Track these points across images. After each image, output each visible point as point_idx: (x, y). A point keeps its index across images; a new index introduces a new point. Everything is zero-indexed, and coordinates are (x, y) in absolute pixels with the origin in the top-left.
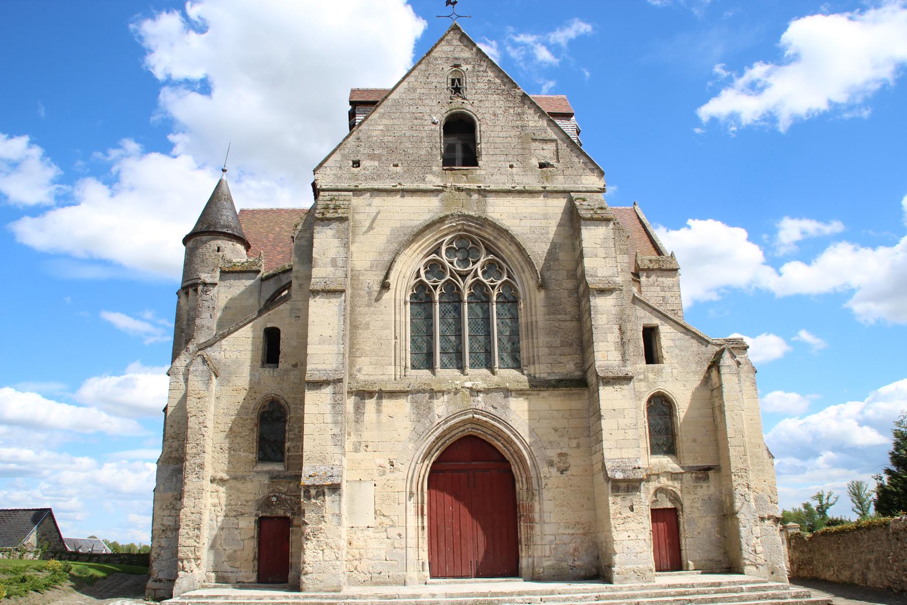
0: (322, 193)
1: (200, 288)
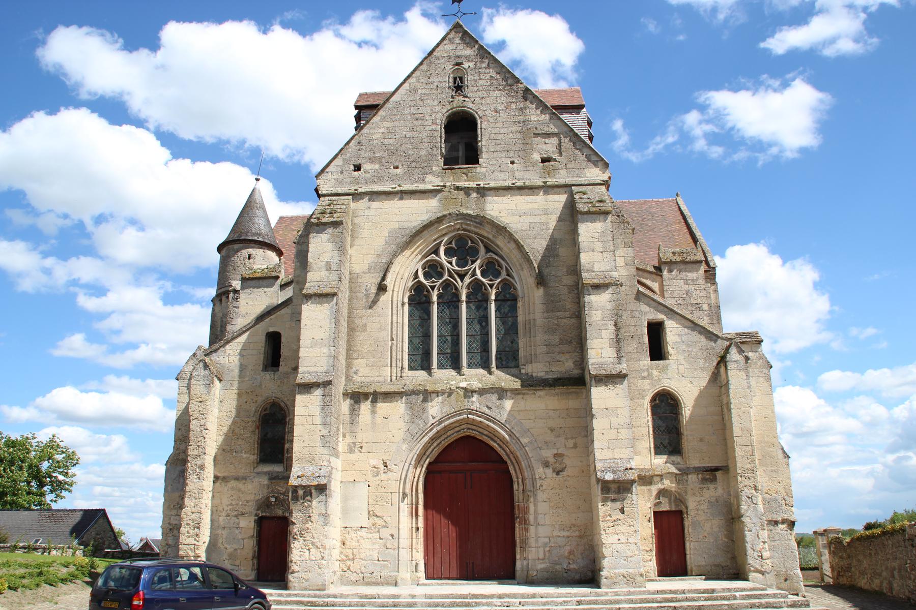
1: (231, 295)
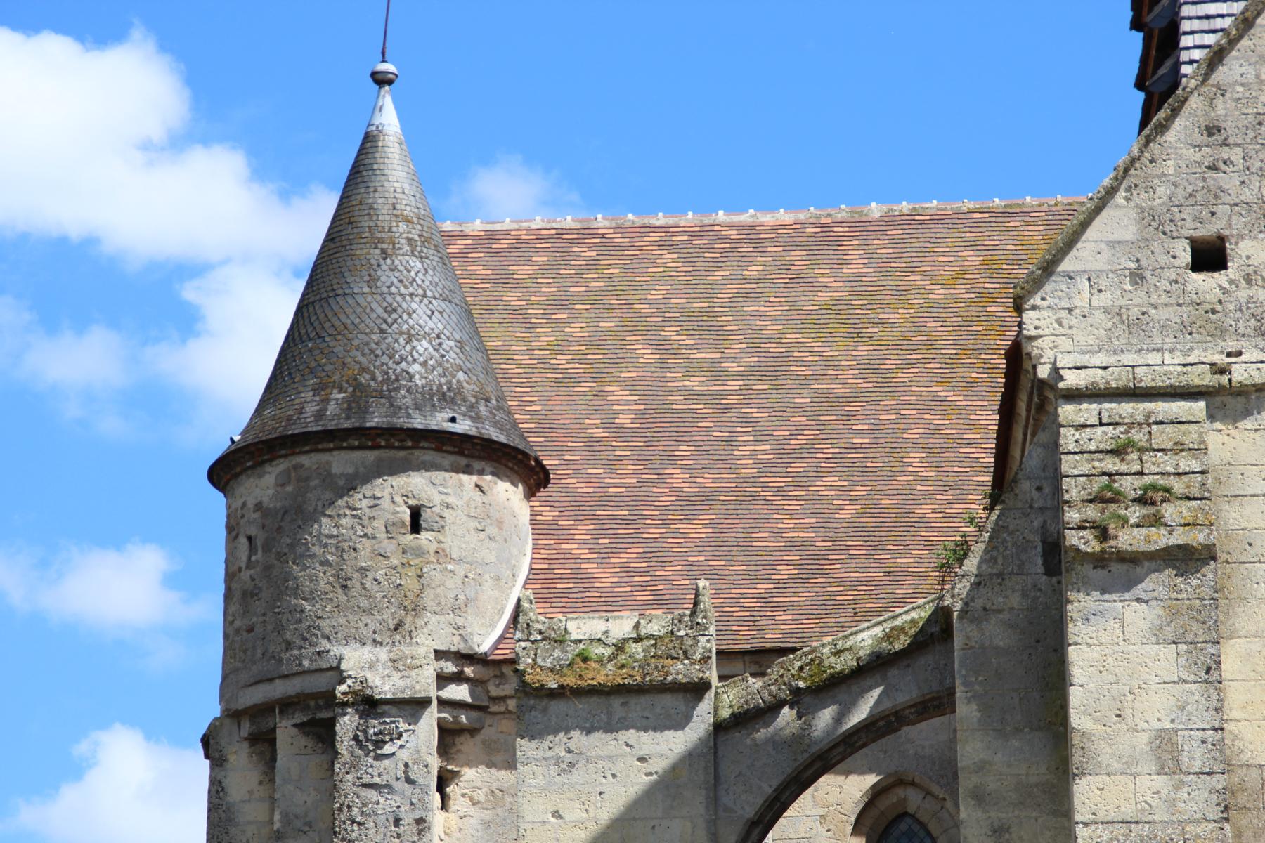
0: (1067, 411)
1: (347, 723)
